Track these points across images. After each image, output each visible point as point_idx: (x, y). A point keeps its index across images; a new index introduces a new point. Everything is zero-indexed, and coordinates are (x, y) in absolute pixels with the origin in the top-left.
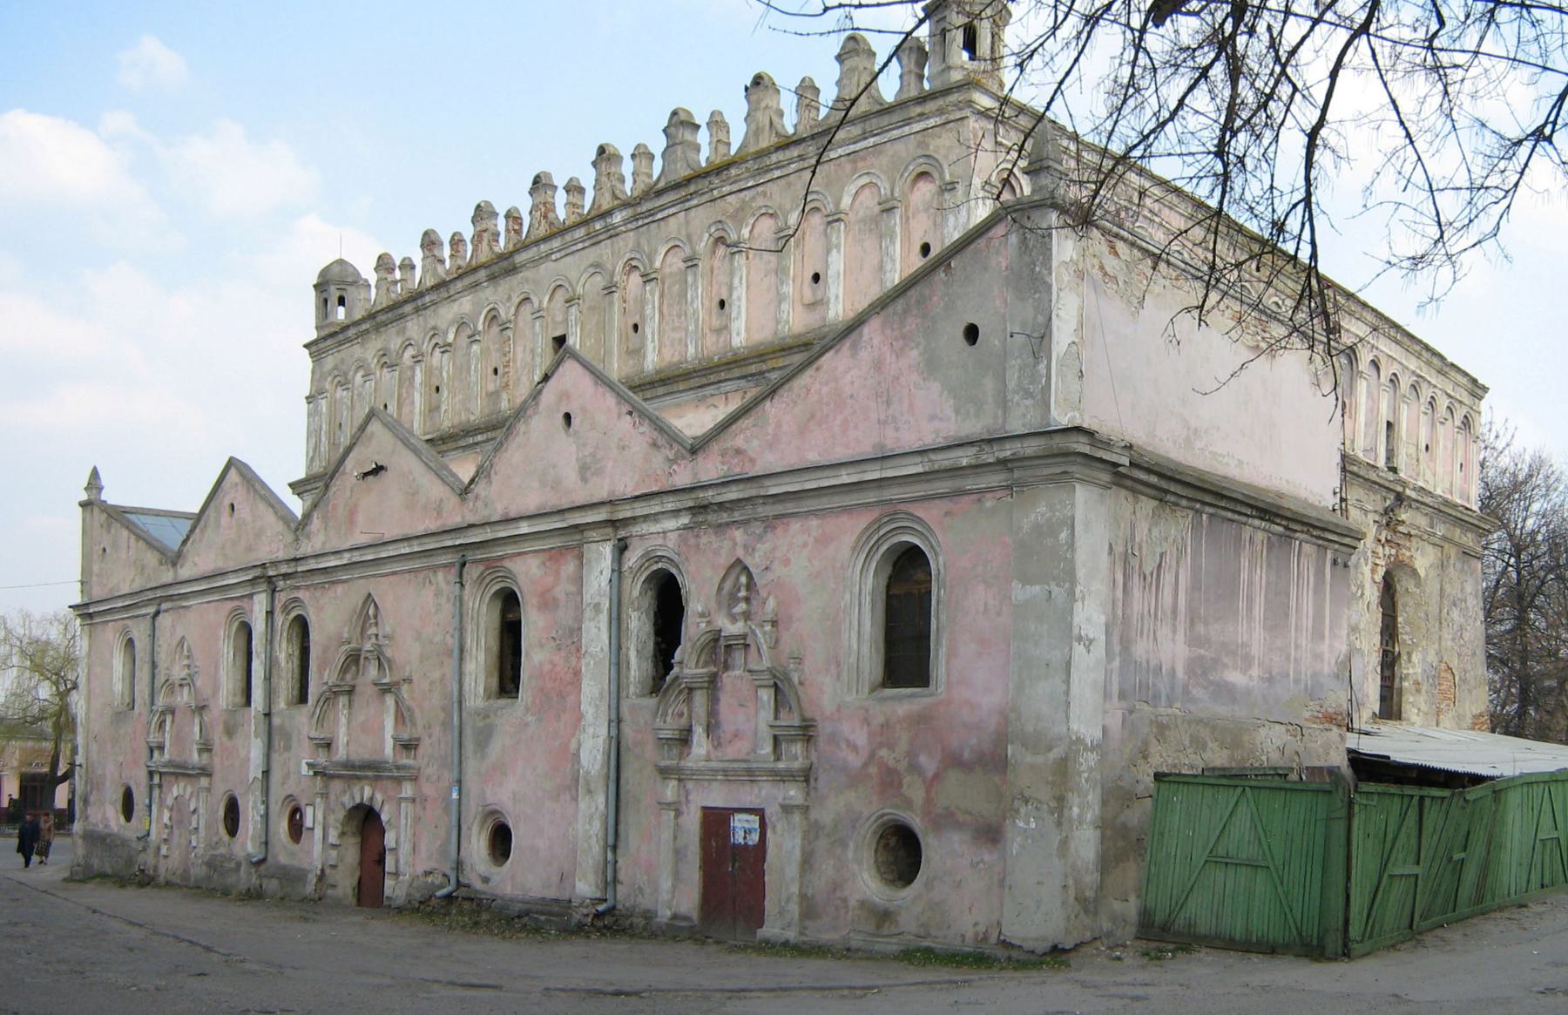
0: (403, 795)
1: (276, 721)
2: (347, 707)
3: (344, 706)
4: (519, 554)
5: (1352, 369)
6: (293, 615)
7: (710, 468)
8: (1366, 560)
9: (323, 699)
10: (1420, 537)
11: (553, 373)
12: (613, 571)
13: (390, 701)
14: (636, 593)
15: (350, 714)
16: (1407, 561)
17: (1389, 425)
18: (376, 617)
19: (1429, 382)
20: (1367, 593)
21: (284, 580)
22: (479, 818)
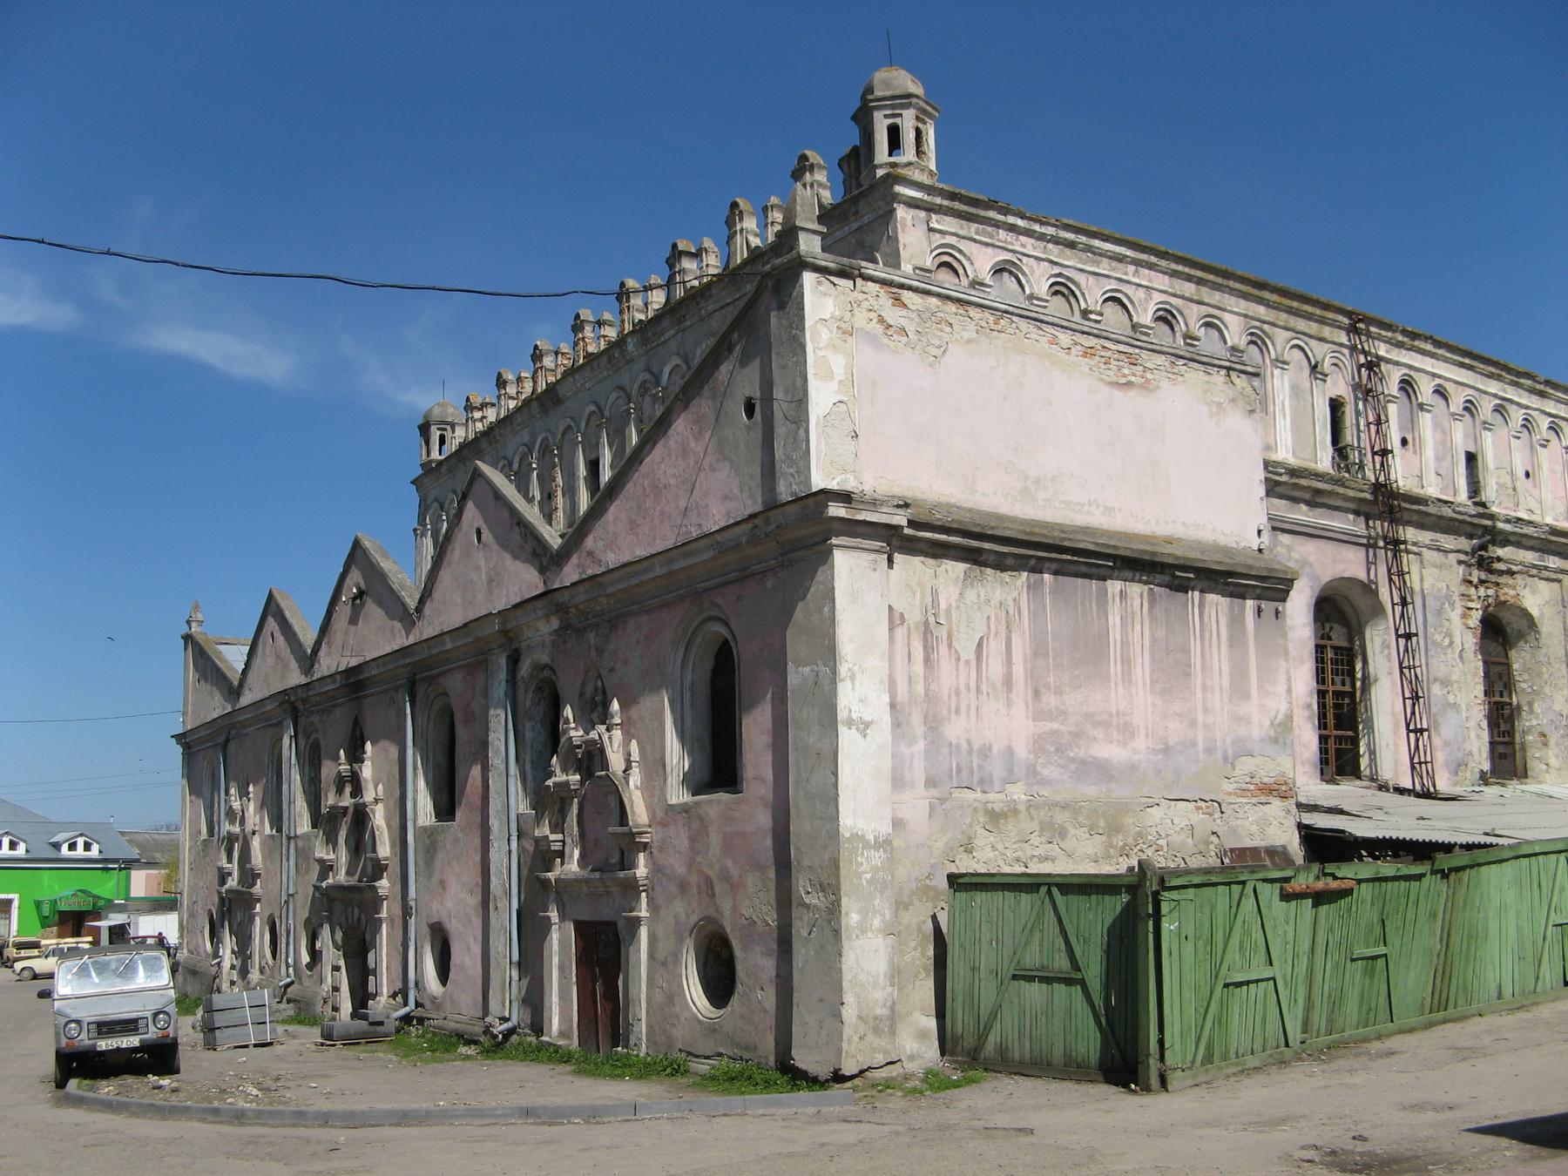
5: (1411, 403)
7: (570, 574)
8: (1452, 605)
10: (1526, 573)
11: (468, 492)
12: (507, 681)
14: (528, 703)
16: (1512, 601)
17: (1471, 458)
19: (1518, 404)
20: (1457, 640)
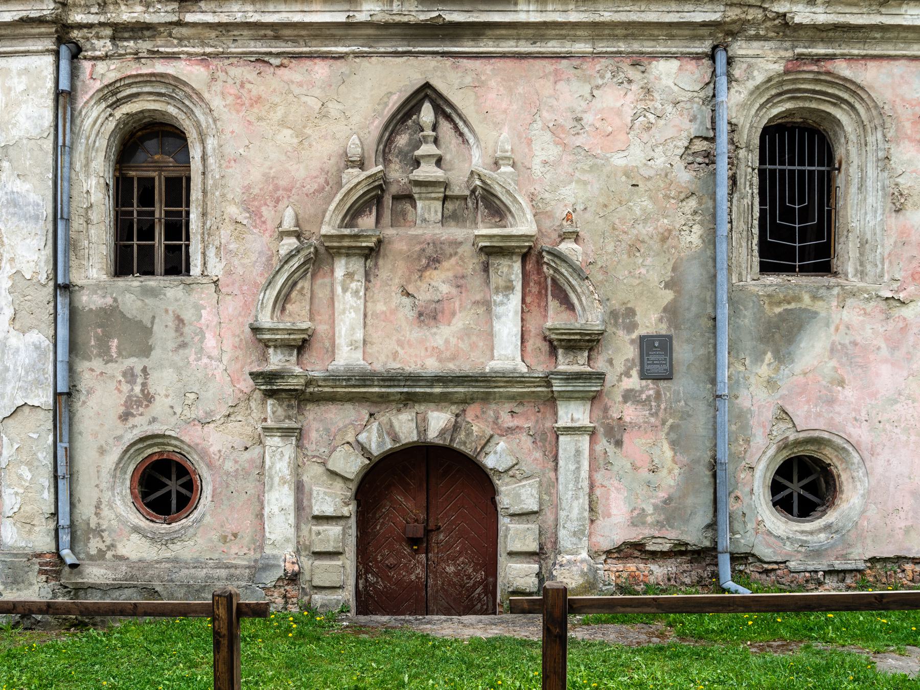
0: (561, 423)
1: (88, 300)
2: (360, 275)
3: (350, 275)
4: (864, 57)
6: (126, 109)
9: (295, 263)
13: (513, 269)
15: (366, 289)
18: (435, 128)
21: (113, 39)
22: (772, 451)
